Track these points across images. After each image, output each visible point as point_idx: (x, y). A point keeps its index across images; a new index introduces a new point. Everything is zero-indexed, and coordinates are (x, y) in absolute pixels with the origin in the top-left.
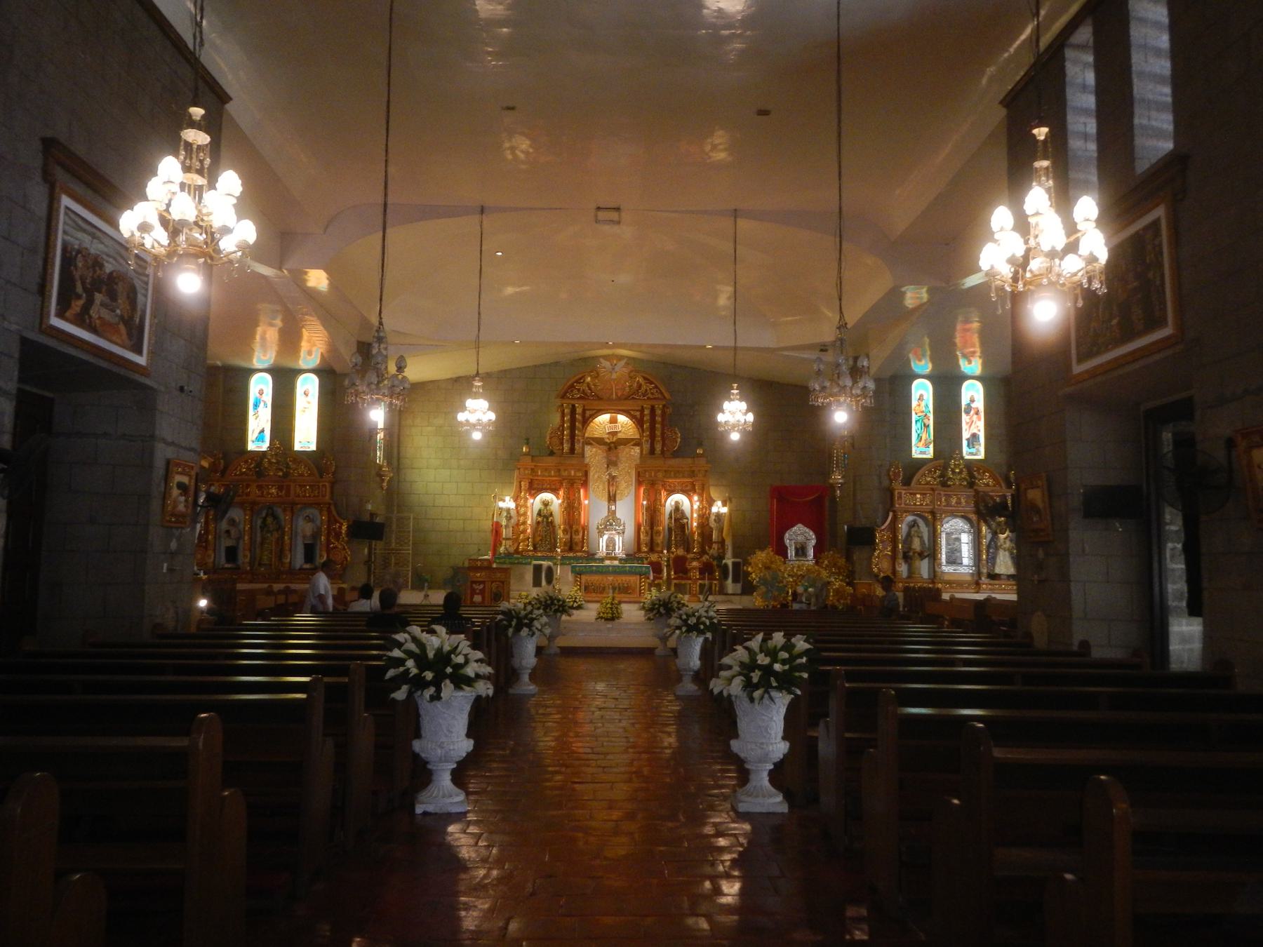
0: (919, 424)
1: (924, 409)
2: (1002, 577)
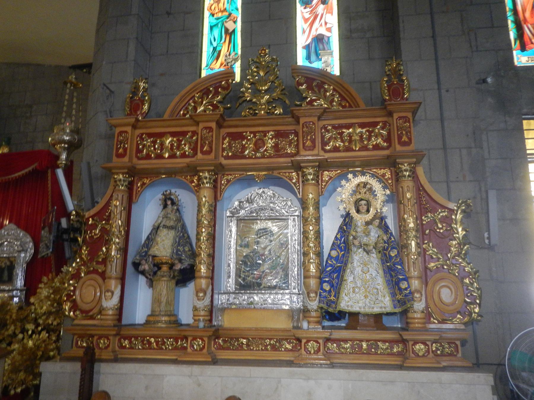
0: (216, 32)
1: (226, 5)
2: (361, 318)
